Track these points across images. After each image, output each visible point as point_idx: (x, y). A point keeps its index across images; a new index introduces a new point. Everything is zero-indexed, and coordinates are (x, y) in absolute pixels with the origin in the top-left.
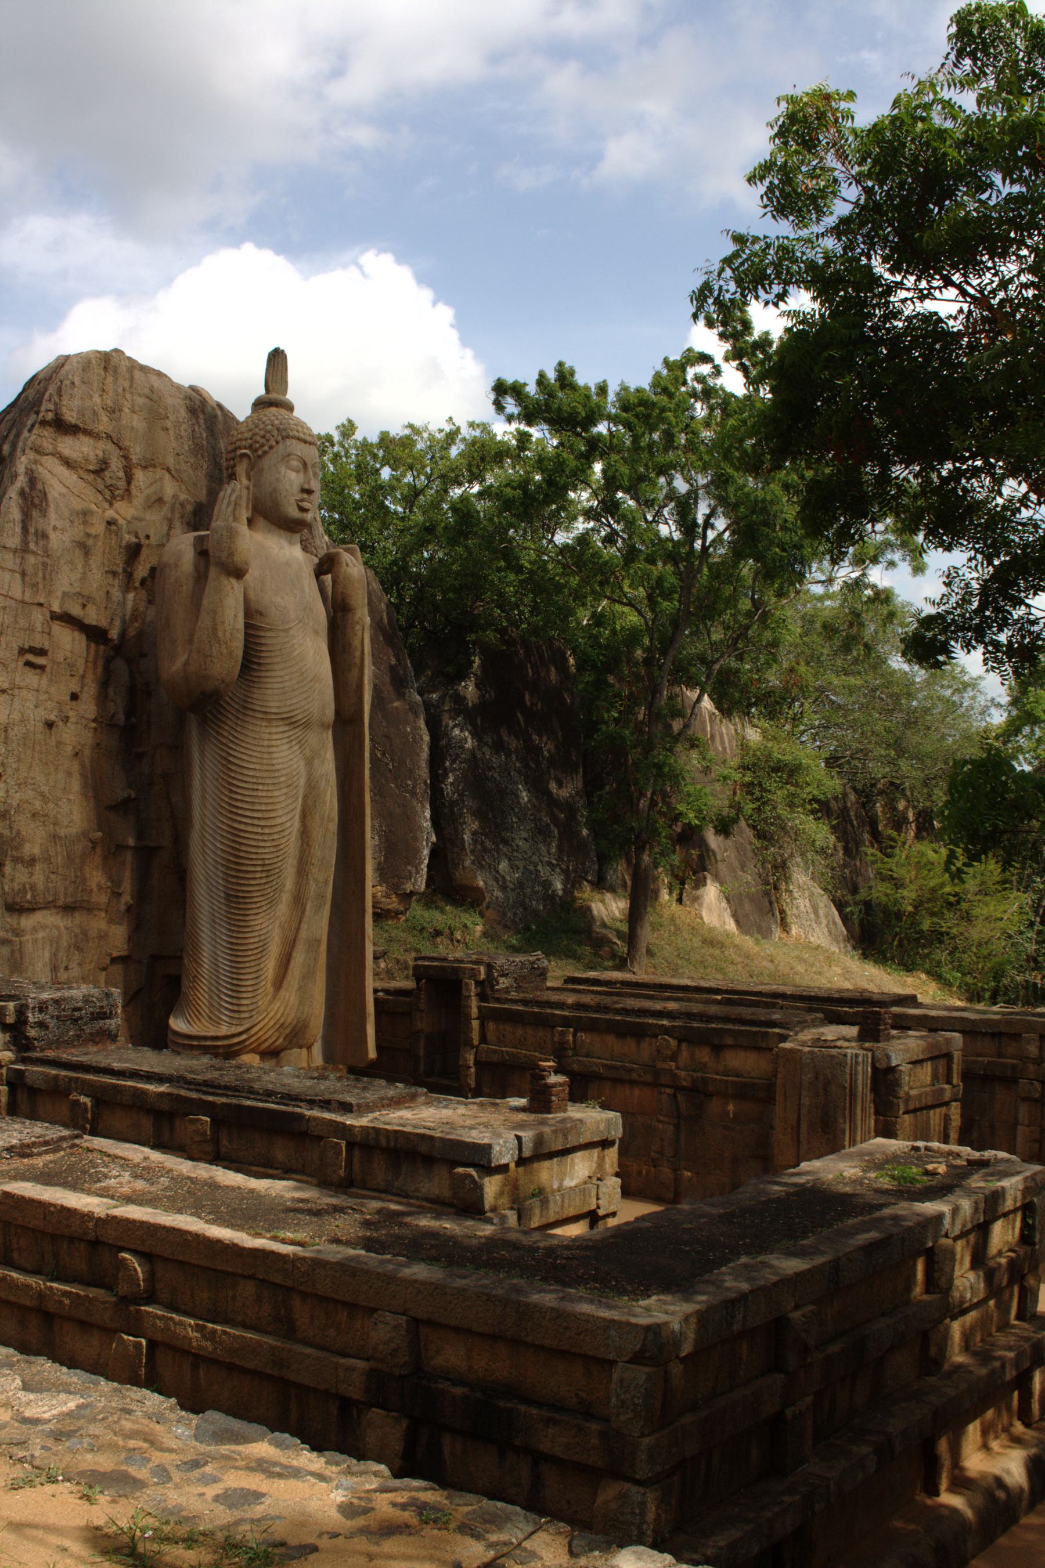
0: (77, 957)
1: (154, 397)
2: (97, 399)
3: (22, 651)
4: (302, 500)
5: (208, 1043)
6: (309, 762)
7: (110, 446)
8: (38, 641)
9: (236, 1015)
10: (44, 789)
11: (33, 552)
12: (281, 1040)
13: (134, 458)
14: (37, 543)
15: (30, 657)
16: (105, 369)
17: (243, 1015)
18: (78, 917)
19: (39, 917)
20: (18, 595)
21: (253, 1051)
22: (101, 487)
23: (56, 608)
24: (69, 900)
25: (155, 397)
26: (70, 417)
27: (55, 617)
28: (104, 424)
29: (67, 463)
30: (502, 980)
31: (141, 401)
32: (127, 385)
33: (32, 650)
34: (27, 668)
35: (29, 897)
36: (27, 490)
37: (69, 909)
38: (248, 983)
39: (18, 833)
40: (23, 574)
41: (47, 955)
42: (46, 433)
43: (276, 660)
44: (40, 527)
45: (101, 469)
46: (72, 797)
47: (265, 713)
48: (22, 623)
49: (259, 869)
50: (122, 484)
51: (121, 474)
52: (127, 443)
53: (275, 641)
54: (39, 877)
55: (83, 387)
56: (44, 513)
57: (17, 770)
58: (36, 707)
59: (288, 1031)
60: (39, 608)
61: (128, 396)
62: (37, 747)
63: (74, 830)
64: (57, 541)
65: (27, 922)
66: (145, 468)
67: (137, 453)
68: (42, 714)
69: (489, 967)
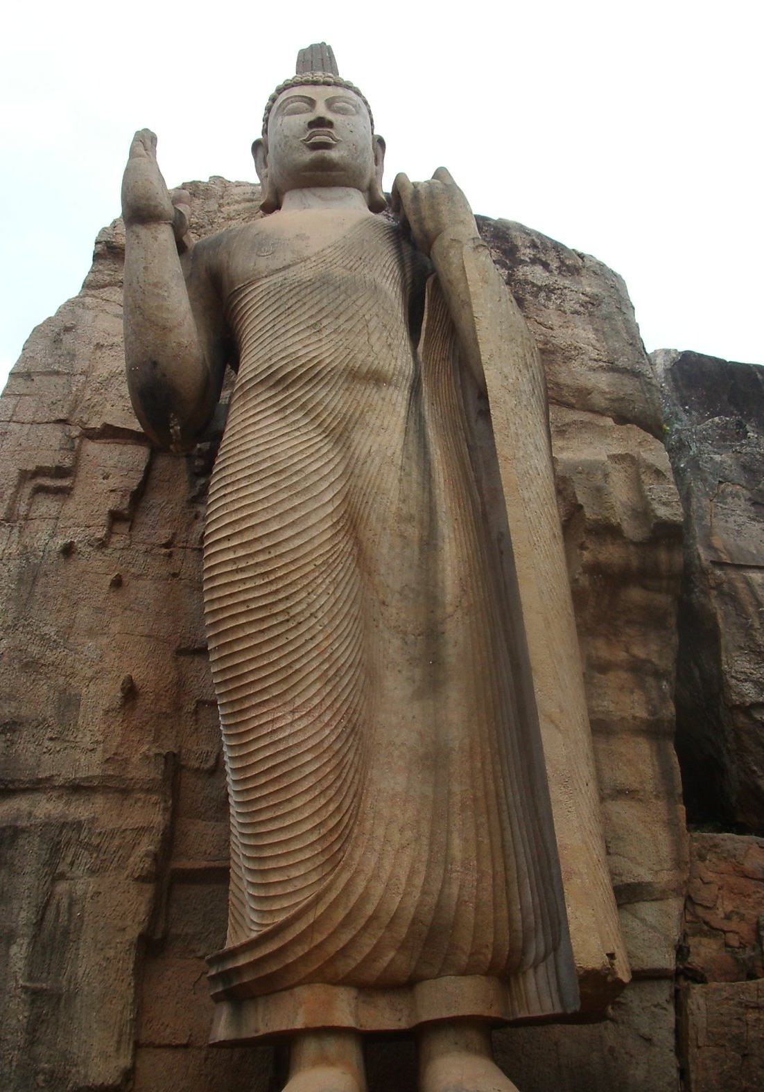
3: (25, 476)
6: (340, 434)
21: (328, 975)
23: (96, 423)
27: (91, 435)
33: (40, 472)
34: (40, 497)
42: (101, 267)
60: (59, 427)
68: (60, 541)
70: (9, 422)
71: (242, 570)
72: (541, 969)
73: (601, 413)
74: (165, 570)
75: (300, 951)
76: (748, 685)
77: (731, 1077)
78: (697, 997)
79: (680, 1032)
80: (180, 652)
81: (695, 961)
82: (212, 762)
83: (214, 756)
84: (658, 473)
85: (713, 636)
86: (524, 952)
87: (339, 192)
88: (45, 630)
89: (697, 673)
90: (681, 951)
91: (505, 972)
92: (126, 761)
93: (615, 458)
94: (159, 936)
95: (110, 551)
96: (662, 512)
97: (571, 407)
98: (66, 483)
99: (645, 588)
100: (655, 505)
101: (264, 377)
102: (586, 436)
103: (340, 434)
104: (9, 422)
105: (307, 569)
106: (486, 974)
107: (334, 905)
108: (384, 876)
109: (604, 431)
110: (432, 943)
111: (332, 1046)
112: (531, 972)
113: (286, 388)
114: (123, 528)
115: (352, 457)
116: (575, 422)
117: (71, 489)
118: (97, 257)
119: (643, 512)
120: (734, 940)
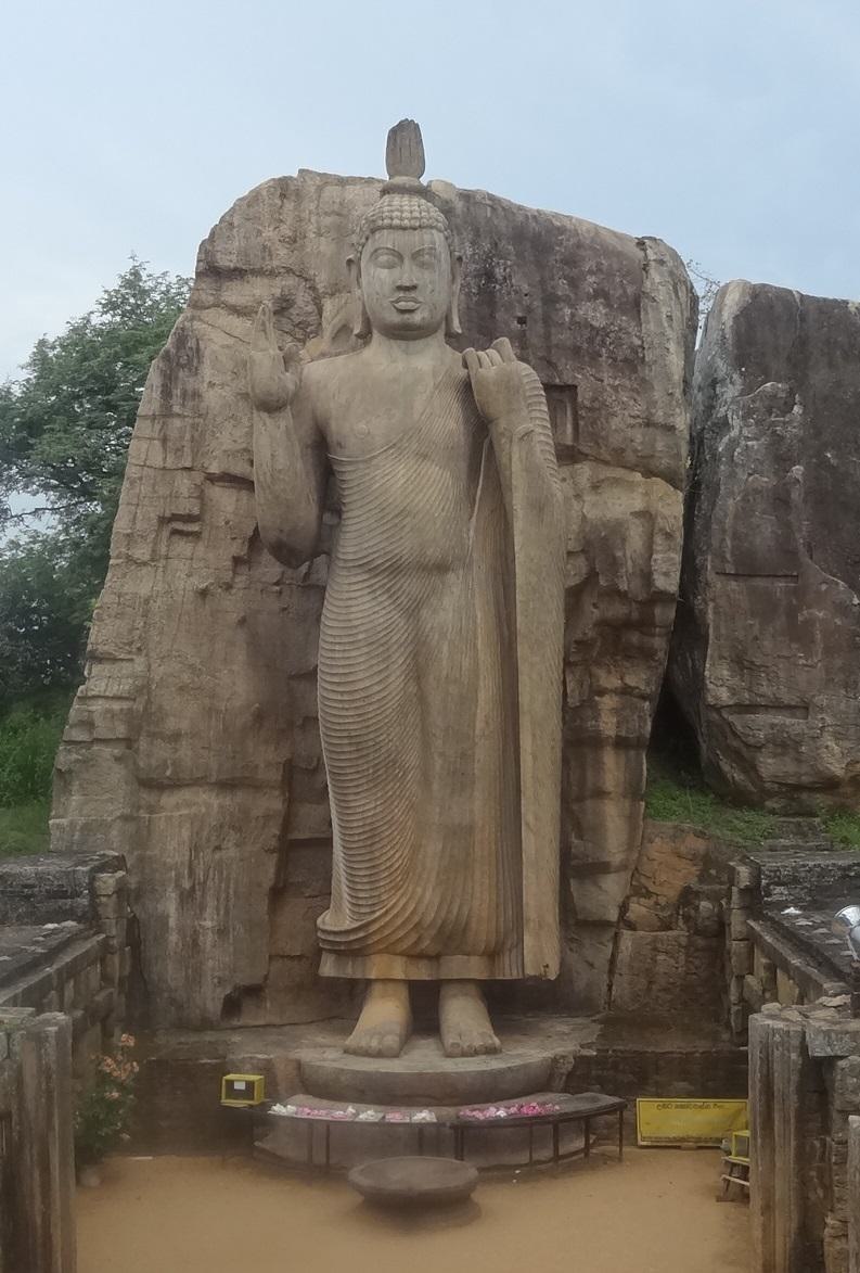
0: (233, 837)
1: (342, 212)
2: (269, 233)
3: (164, 520)
4: (397, 301)
5: (331, 938)
6: (413, 611)
7: (291, 281)
8: (188, 506)
9: (356, 910)
10: (196, 661)
11: (179, 415)
12: (427, 943)
13: (321, 287)
14: (183, 405)
15: (179, 526)
16: (283, 196)
17: (363, 910)
18: (240, 796)
19: (186, 794)
20: (158, 462)
21: (390, 950)
22: (288, 327)
23: (214, 468)
24: (223, 777)
25: (345, 212)
26: (226, 261)
27: (211, 478)
28: (282, 256)
29: (236, 310)
30: (778, 889)
31: (328, 220)
32: (312, 207)
33: (175, 518)
34: (176, 538)
35: (168, 773)
36: (173, 351)
37: (227, 785)
38: (361, 873)
39: (161, 707)
40: (164, 440)
41: (186, 834)
43: (355, 497)
44: (189, 388)
45: (283, 306)
46: (235, 668)
47: (345, 561)
48: (162, 491)
49: (346, 741)
50: (313, 319)
51: (310, 308)
52: (312, 272)
53: (354, 476)
54: (185, 752)
55: (248, 224)
56: (196, 372)
57: (159, 643)
58: (188, 576)
59: (433, 932)
61: (313, 219)
62: (185, 618)
63: (238, 703)
64: (212, 399)
65: (168, 800)
66: (332, 295)
67: (323, 280)
69: (757, 873)
70: (144, 466)
71: (347, 709)
72: (514, 951)
73: (632, 469)
74: (276, 606)
75: (376, 938)
76: (724, 689)
77: (638, 995)
78: (627, 937)
79: (612, 961)
80: (292, 677)
81: (630, 915)
82: (315, 763)
83: (315, 759)
84: (669, 536)
85: (703, 640)
86: (504, 943)
87: (420, 344)
88: (192, 661)
89: (690, 665)
90: (624, 908)
91: (492, 955)
92: (257, 767)
93: (637, 514)
94: (281, 885)
95: (234, 591)
96: (661, 582)
97: (606, 463)
98: (194, 527)
99: (642, 632)
100: (655, 576)
101: (361, 563)
102: (614, 490)
103: (413, 611)
104: (144, 466)
105: (388, 713)
106: (482, 955)
107: (396, 916)
108: (426, 901)
109: (631, 486)
110: (451, 938)
111: (391, 987)
112: (508, 953)
113: (378, 575)
114: (243, 569)
115: (419, 630)
116: (607, 479)
117: (201, 533)
118: (198, 274)
119: (647, 577)
120: (663, 901)
